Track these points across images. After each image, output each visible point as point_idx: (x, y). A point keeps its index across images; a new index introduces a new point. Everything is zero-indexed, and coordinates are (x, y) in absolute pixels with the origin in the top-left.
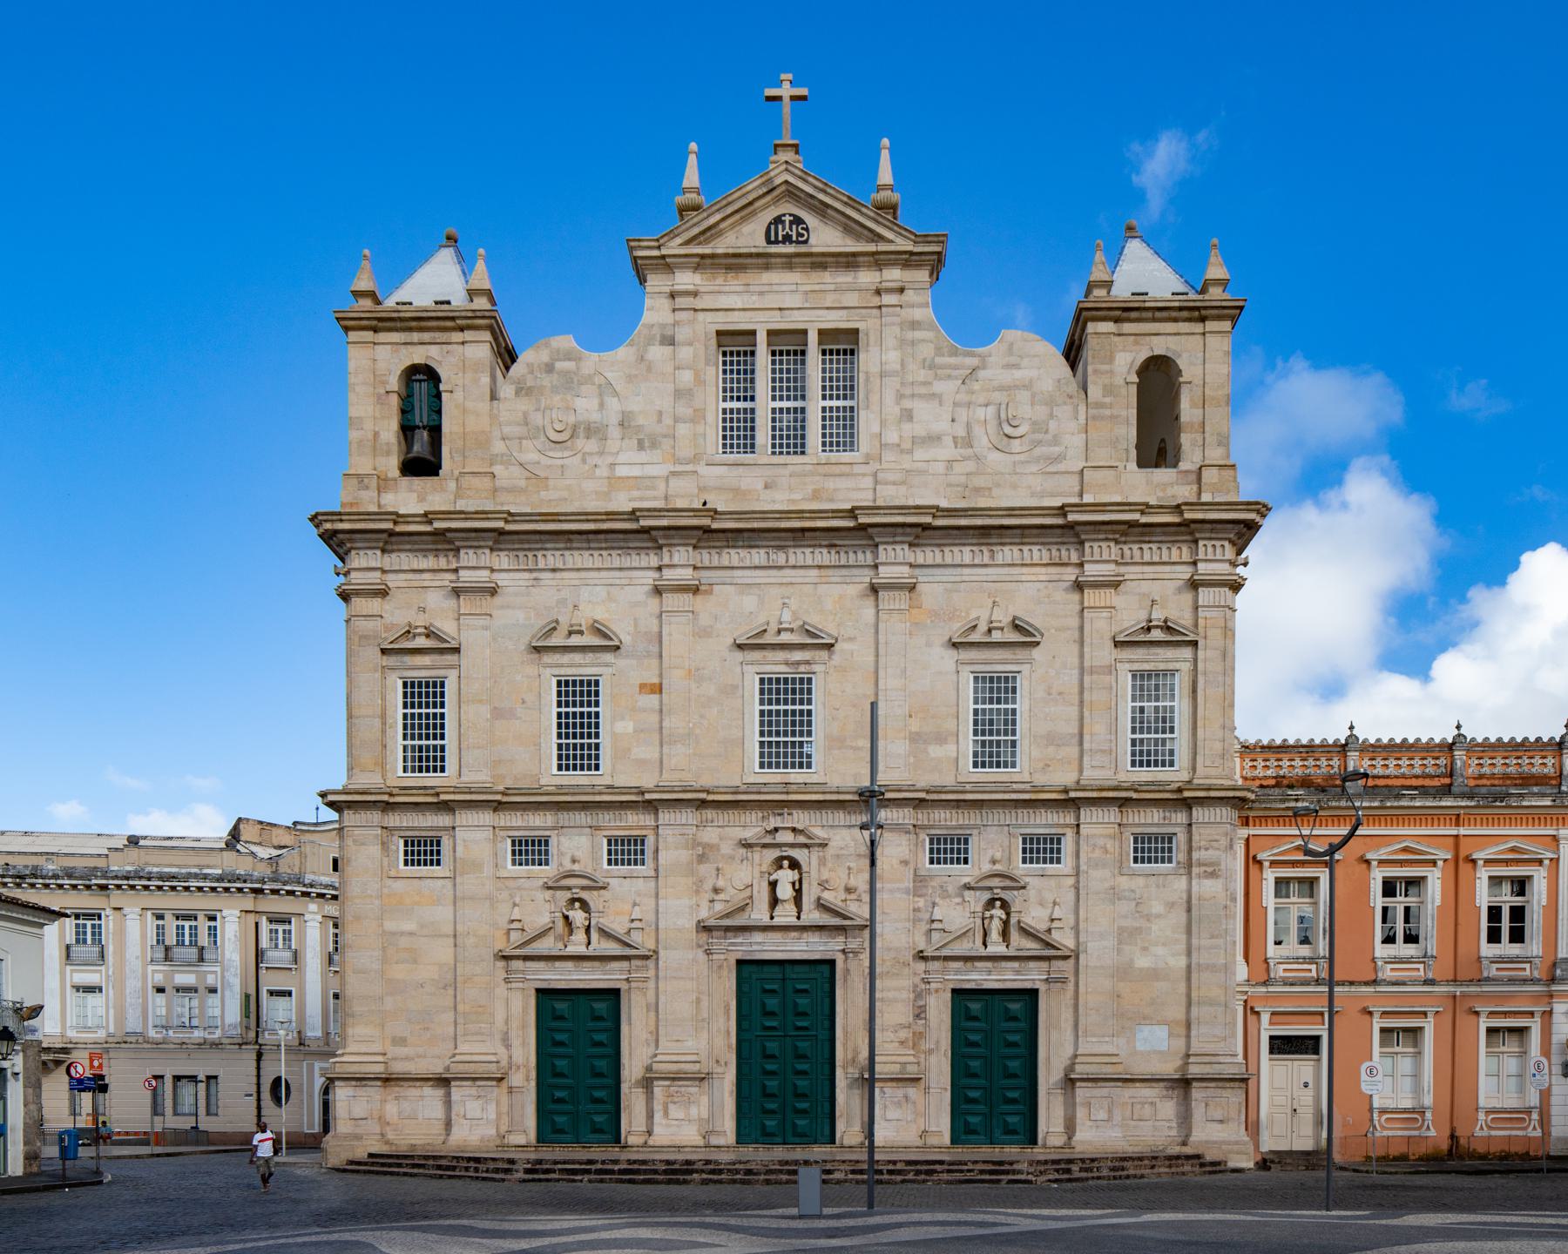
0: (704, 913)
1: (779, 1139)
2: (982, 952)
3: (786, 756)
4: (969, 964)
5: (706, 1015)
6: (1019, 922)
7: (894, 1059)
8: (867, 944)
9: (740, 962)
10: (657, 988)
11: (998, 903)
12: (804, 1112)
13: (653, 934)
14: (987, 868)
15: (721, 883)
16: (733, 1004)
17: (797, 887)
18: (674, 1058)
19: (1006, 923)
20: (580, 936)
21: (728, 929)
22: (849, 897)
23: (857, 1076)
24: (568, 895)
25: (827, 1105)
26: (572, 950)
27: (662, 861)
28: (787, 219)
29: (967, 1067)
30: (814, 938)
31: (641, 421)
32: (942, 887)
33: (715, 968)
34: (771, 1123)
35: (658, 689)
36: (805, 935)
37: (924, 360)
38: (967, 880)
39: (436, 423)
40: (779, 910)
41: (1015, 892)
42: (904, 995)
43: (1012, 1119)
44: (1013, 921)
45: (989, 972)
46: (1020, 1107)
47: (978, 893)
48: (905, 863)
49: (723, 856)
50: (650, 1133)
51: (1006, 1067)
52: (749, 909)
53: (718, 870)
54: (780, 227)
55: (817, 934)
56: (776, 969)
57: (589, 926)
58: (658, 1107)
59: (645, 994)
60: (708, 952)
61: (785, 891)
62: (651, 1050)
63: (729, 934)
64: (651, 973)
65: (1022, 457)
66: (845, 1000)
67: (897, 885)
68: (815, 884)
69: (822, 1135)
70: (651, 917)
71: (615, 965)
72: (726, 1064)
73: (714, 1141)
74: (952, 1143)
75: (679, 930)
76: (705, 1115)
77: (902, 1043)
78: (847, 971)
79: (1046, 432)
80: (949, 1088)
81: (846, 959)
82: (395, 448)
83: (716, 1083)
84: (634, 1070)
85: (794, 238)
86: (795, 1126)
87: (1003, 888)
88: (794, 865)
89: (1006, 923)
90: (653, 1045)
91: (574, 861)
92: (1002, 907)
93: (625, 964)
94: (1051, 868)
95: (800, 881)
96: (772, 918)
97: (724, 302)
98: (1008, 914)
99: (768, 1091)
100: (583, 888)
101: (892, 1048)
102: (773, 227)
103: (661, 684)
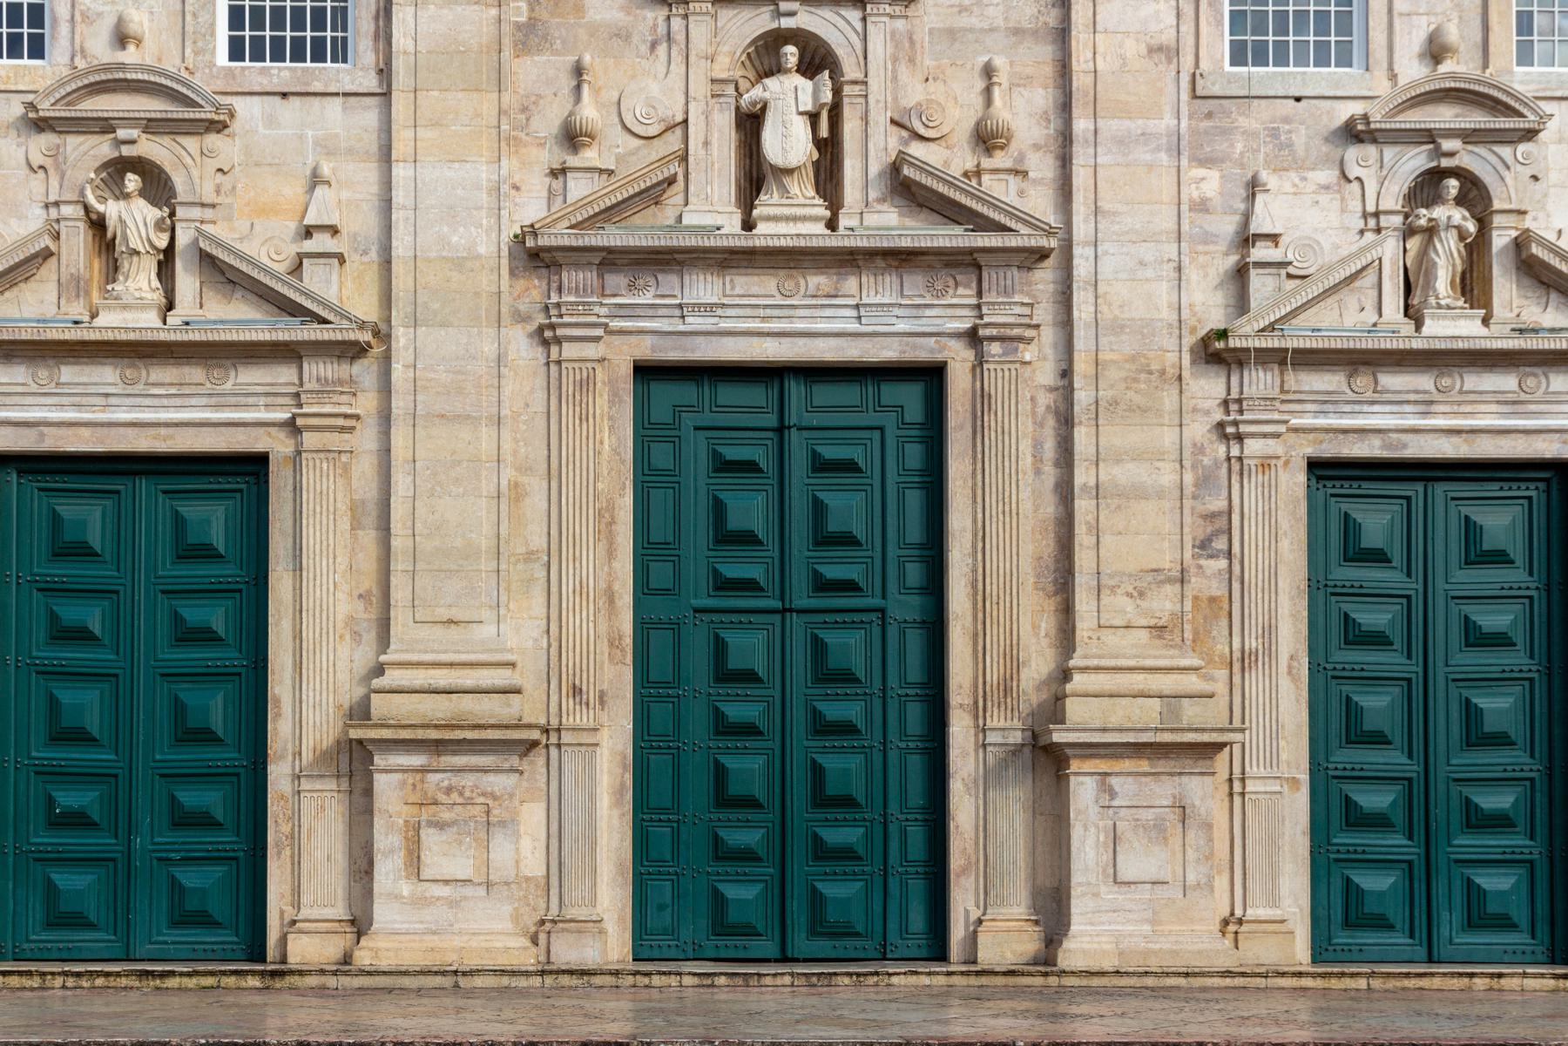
0: (530, 208)
1: (769, 947)
2: (1404, 337)
4: (1362, 381)
5: (539, 542)
6: (1520, 244)
7: (1139, 681)
8: (1045, 313)
9: (645, 372)
10: (386, 451)
11: (1453, 185)
12: (846, 854)
13: (372, 277)
14: (1412, 71)
15: (589, 112)
16: (627, 501)
18: (441, 678)
19: (1476, 249)
20: (141, 280)
21: (610, 260)
22: (987, 163)
23: (1016, 738)
24: (103, 149)
25: (917, 836)
26: (113, 323)
27: (401, 39)
29: (1351, 711)
30: (880, 290)
32: (1274, 133)
33: (568, 387)
34: (743, 893)
36: (851, 284)
38: (1357, 108)
40: (768, 203)
41: (1505, 151)
42: (1167, 476)
43: (1495, 882)
44: (1500, 240)
45: (1426, 404)
46: (1516, 841)
47: (1389, 152)
48: (1170, 52)
49: (593, 30)
50: (359, 925)
51: (1471, 713)
52: (674, 197)
53: (578, 71)
55: (890, 280)
56: (755, 395)
57: (169, 251)
58: (387, 840)
59: (346, 469)
60: (546, 337)
62: (364, 655)
63: (616, 280)
64: (366, 404)
66: (977, 497)
67: (1136, 125)
68: (879, 119)
69: (904, 930)
70: (360, 222)
71: (252, 376)
72: (602, 695)
73: (567, 952)
74: (1316, 958)
75: (458, 264)
76: (534, 865)
77: (1159, 630)
78: (981, 400)
80: (1305, 777)
81: (980, 361)
83: (572, 762)
84: (309, 715)
86: (816, 901)
87: (1471, 137)
88: (816, 60)
89: (1476, 249)
90: (370, 637)
91: (122, 39)
92: (1460, 201)
93: (284, 375)
95: (835, 111)
96: (748, 225)
99: (734, 789)
100: (153, 126)
101: (1132, 645)
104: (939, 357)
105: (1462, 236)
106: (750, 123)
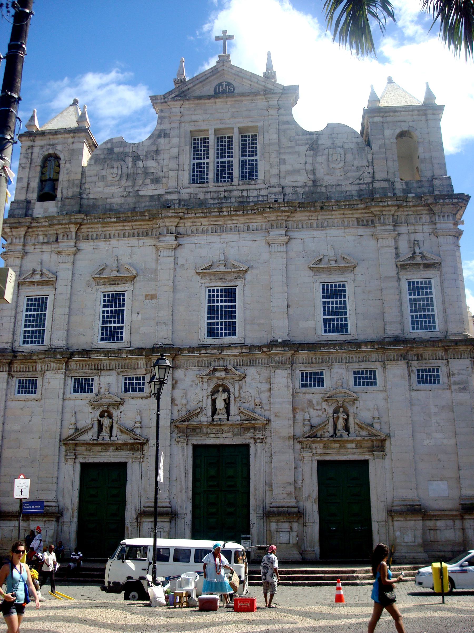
3: (217, 330)
11: (341, 410)
16: (191, 471)
17: (227, 401)
28: (224, 83)
31: (152, 170)
35: (153, 297)
37: (290, 137)
39: (55, 178)
54: (221, 87)
61: (220, 405)
65: (341, 178)
79: (353, 166)
82: (36, 190)
85: (227, 91)
88: (226, 390)
89: (347, 420)
92: (343, 412)
94: (370, 388)
95: (229, 398)
96: (213, 420)
97: (194, 118)
98: (348, 415)
102: (217, 87)
103: (156, 294)
104: (247, 443)
105: (344, 419)
106: (214, 401)
